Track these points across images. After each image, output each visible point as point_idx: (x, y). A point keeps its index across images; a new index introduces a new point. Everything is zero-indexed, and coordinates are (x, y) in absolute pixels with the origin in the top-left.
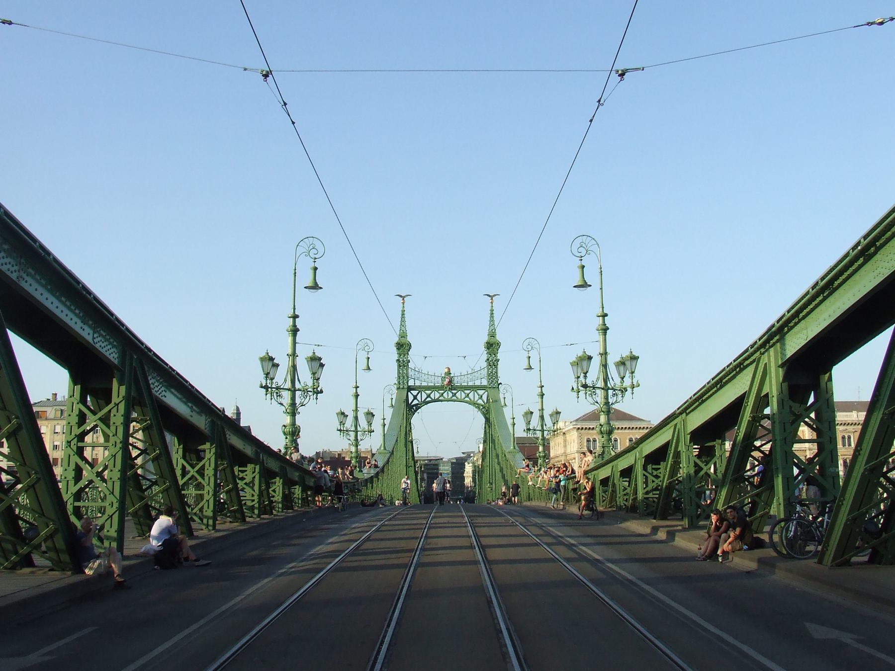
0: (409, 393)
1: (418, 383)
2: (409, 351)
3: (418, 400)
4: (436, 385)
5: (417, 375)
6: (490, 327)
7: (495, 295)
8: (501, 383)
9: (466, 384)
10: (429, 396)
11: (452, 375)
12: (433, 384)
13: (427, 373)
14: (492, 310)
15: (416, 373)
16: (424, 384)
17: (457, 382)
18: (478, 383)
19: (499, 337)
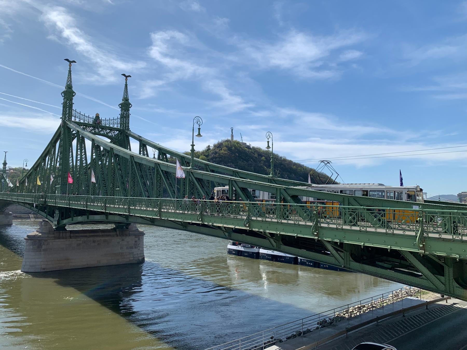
1: (77, 120)
5: (77, 115)
7: (130, 76)
9: (108, 126)
11: (100, 119)
12: (87, 122)
16: (82, 121)
17: (103, 123)
18: (115, 126)
19: (130, 101)
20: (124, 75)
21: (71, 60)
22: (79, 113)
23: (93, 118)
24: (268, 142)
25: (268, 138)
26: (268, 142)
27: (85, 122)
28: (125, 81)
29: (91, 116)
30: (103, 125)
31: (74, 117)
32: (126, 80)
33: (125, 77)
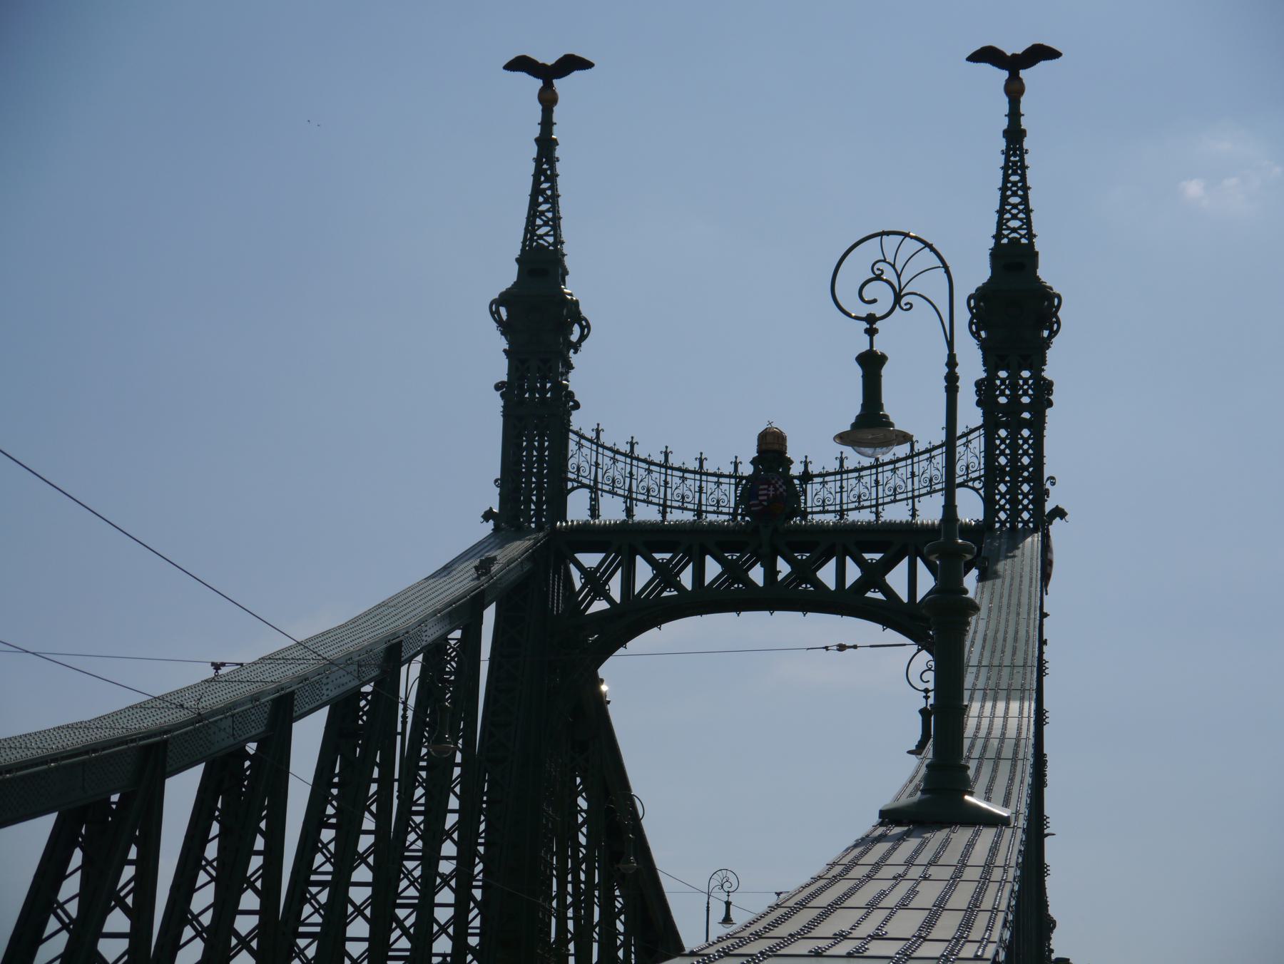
0: (572, 567)
1: (612, 511)
2: (576, 347)
3: (609, 599)
4: (712, 517)
6: (1001, 224)
7: (1040, 53)
8: (1059, 513)
9: (866, 516)
10: (666, 575)
11: (796, 470)
12: (689, 516)
13: (659, 458)
14: (1015, 135)
15: (605, 461)
16: (646, 514)
20: (987, 55)
21: (548, 57)
22: (625, 448)
23: (735, 477)
24: (871, 363)
25: (871, 319)
26: (871, 363)
27: (675, 516)
28: (1006, 100)
29: (719, 462)
30: (817, 518)
31: (587, 491)
32: (1014, 91)
33: (1005, 74)
